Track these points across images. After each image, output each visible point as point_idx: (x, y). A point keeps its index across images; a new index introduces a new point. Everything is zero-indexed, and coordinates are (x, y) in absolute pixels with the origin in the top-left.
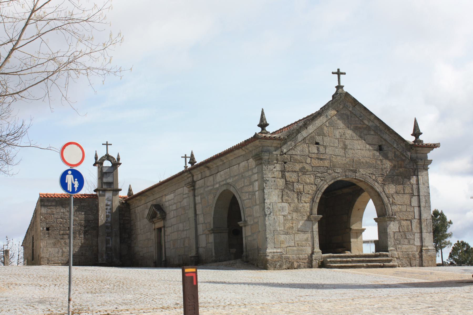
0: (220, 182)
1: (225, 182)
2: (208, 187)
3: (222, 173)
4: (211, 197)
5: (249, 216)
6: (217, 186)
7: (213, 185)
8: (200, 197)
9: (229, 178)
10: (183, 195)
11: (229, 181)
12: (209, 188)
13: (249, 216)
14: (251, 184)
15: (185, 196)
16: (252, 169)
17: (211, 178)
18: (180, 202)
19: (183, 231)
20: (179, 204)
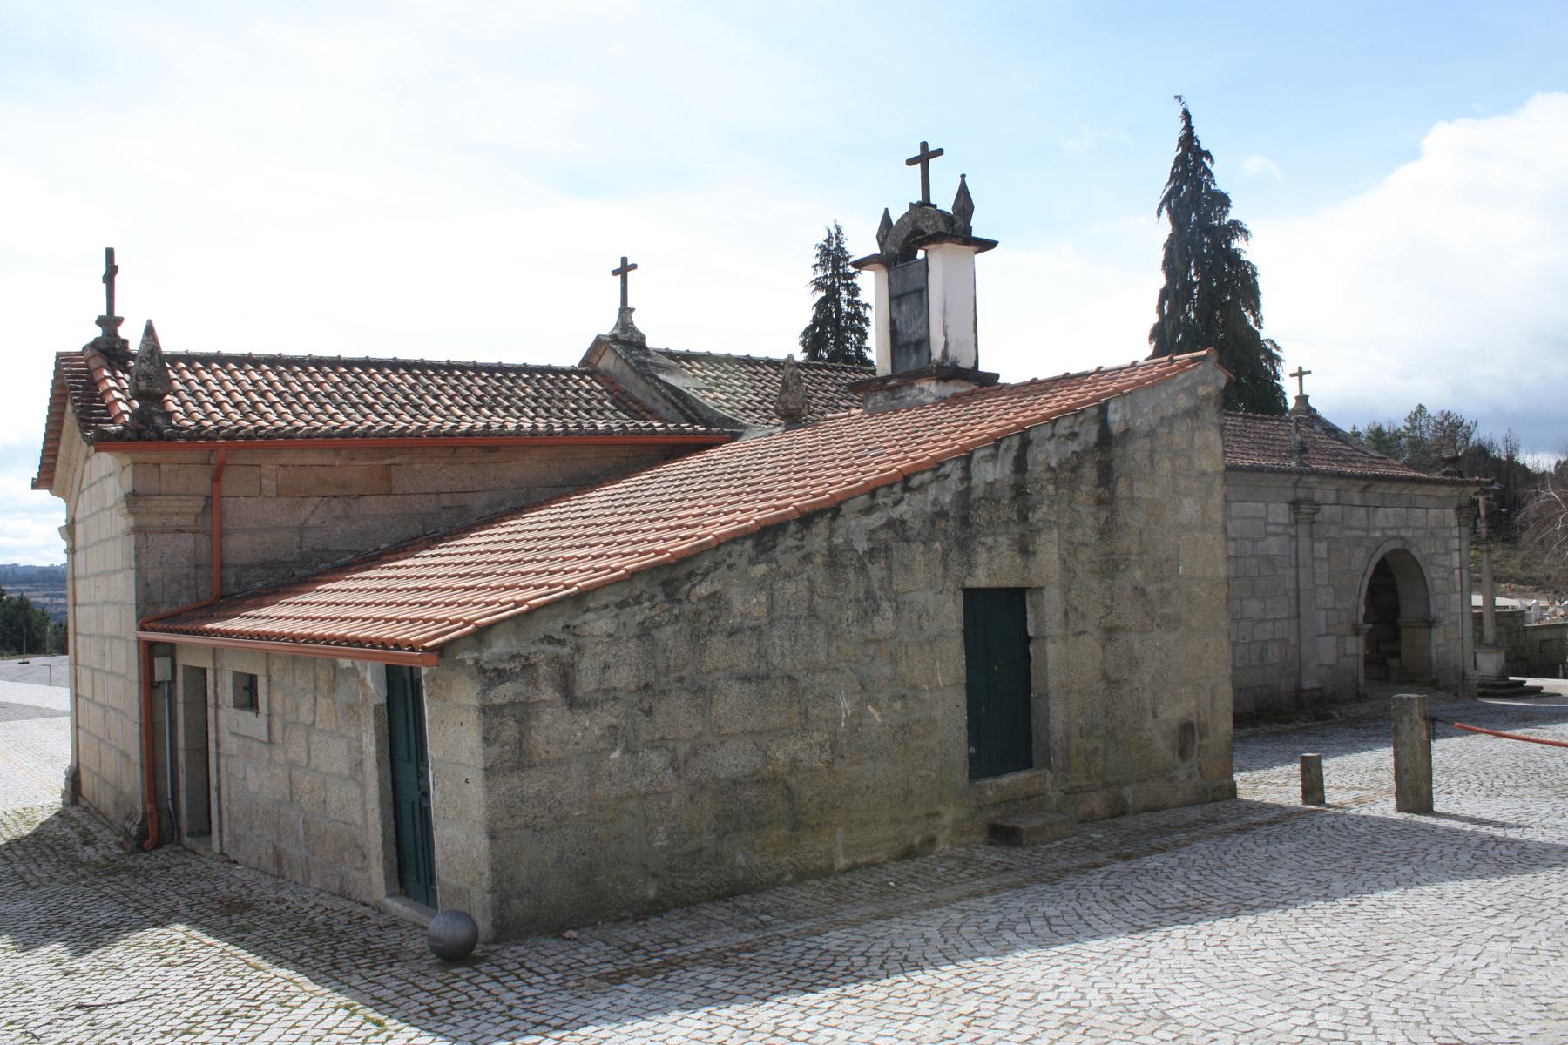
0: (1383, 529)
1: (1395, 533)
2: (1352, 528)
3: (1390, 511)
4: (1360, 554)
5: (1442, 609)
6: (1378, 534)
7: (1367, 530)
8: (1325, 544)
9: (1407, 527)
10: (1267, 523)
11: (1403, 533)
12: (1355, 533)
13: (1442, 609)
14: (1448, 552)
15: (1271, 528)
16: (1450, 528)
17: (1362, 512)
18: (1254, 541)
19: (1262, 621)
20: (1249, 544)
